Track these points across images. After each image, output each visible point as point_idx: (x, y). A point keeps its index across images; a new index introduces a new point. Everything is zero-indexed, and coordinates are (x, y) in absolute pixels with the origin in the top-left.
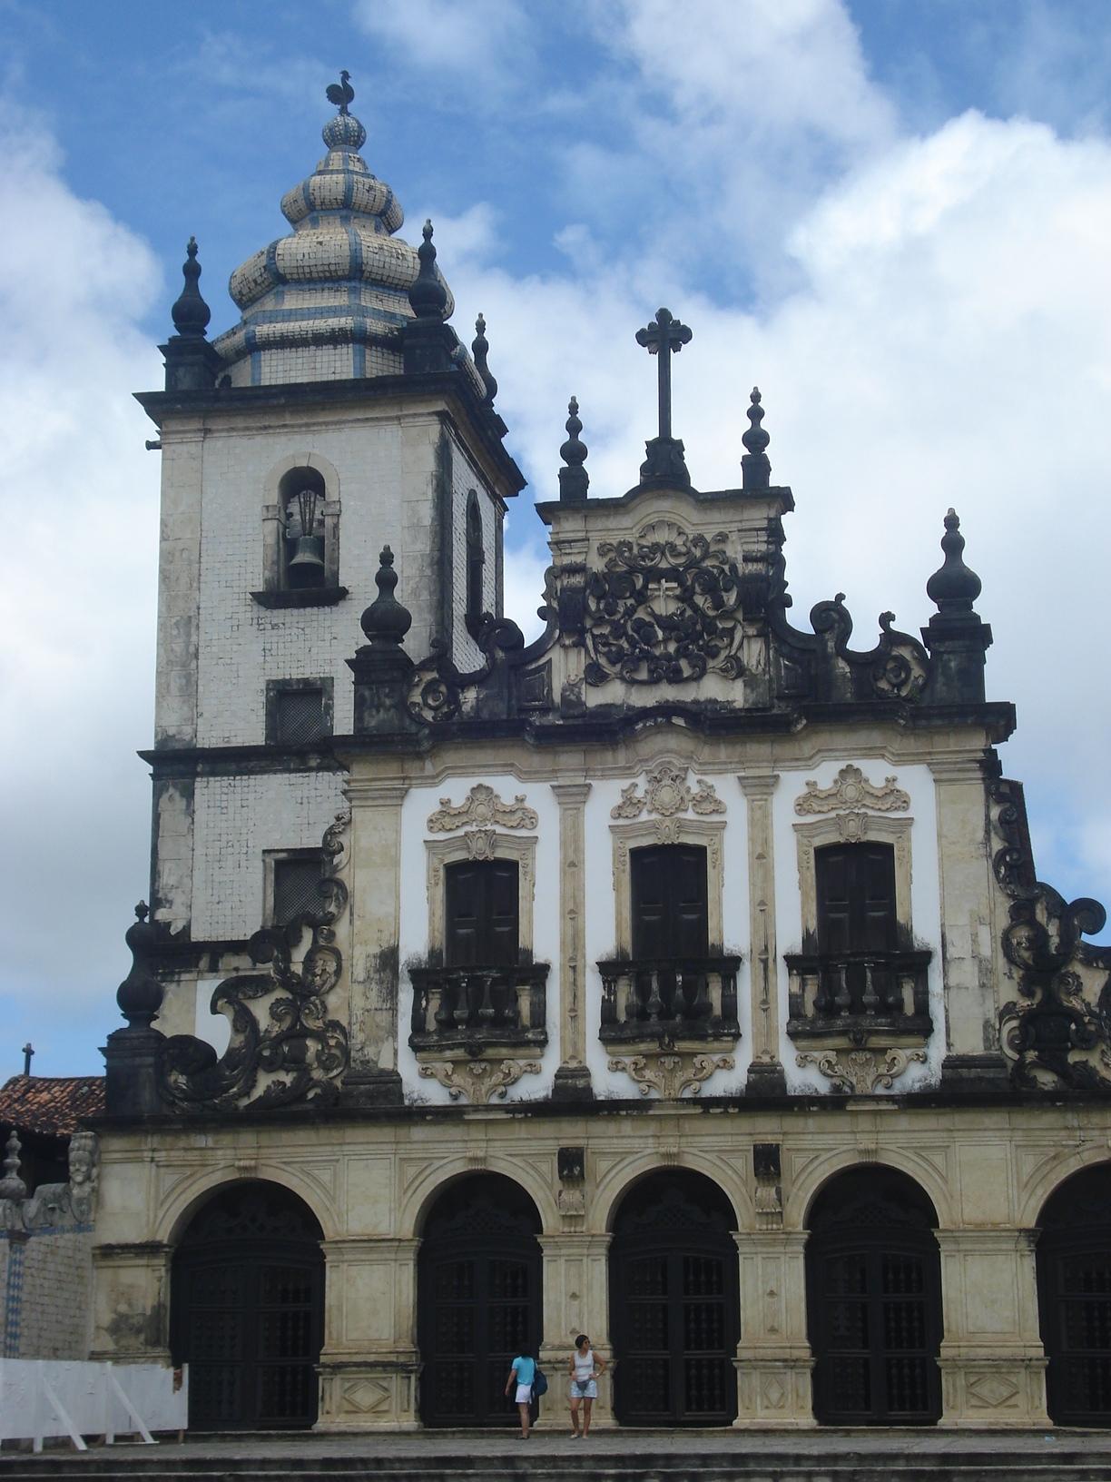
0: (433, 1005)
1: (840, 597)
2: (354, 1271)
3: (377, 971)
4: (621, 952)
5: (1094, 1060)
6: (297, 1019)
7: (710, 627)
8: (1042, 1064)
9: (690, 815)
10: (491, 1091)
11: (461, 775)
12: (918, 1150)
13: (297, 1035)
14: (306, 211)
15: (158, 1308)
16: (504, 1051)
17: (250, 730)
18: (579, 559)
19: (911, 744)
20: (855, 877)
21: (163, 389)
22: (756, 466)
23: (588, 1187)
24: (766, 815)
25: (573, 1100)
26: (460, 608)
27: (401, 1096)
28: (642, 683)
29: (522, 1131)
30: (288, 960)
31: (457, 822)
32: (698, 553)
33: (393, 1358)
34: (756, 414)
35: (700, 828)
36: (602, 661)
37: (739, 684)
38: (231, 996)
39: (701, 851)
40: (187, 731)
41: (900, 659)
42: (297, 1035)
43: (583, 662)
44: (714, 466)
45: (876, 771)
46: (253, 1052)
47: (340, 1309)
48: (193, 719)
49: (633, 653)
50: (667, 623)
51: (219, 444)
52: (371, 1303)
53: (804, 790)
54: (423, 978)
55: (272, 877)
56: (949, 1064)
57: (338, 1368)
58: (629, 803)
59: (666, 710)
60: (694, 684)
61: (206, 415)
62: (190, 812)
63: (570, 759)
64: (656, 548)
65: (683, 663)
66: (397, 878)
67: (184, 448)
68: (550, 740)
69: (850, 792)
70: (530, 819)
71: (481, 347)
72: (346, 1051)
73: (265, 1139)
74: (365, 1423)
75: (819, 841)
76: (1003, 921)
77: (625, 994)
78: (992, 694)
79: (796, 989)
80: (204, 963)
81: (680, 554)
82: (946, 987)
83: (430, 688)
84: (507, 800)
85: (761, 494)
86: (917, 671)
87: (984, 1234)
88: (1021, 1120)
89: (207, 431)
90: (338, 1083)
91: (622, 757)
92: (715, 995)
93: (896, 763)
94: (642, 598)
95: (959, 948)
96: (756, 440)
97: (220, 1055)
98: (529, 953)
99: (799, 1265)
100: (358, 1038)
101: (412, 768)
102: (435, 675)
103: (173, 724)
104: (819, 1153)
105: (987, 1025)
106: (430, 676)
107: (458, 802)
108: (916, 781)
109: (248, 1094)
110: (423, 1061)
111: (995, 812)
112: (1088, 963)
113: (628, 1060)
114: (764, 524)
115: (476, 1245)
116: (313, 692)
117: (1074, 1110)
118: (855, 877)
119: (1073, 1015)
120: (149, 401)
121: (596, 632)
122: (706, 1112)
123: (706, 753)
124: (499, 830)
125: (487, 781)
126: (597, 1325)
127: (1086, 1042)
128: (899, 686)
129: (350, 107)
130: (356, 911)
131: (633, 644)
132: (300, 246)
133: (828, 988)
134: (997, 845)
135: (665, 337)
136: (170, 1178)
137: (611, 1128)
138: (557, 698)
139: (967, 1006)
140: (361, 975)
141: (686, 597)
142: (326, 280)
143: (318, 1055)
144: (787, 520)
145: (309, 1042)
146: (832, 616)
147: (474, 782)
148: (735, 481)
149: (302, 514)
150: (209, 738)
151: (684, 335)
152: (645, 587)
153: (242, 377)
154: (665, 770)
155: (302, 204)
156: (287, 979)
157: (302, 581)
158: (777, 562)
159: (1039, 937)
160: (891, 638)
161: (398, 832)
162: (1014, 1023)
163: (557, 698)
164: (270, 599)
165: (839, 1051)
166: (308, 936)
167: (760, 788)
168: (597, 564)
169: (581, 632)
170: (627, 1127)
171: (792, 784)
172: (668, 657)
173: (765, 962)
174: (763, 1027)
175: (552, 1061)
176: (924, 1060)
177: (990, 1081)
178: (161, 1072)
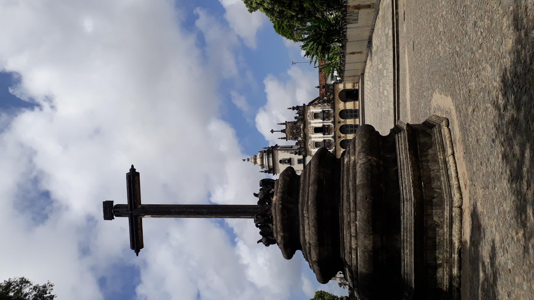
14: (255, 162)
22: (283, 124)
44: (284, 127)
45: (308, 114)
63: (307, 138)
85: (285, 124)
87: (345, 106)
96: (281, 124)
108: (309, 111)
120: (274, 175)
127: (329, 99)
139: (328, 108)
146: (296, 118)
158: (291, 122)
160: (298, 113)
171: (309, 121)
174: (329, 123)
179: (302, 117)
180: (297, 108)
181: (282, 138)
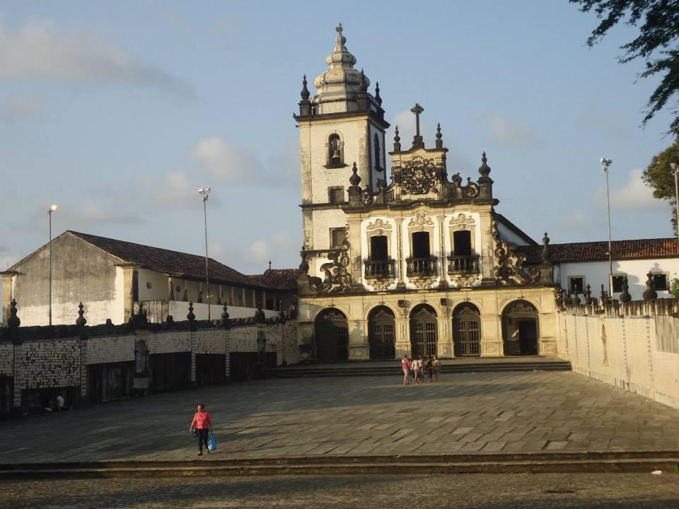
0: (370, 268)
5: (514, 278)
7: (429, 180)
10: (383, 288)
13: (339, 276)
15: (313, 336)
17: (324, 198)
19: (475, 207)
20: (462, 239)
22: (439, 143)
25: (402, 290)
26: (374, 165)
29: (390, 296)
30: (337, 259)
34: (439, 129)
39: (427, 234)
42: (339, 276)
44: (430, 142)
45: (468, 214)
46: (330, 280)
50: (418, 179)
54: (367, 263)
56: (482, 280)
59: (418, 203)
60: (425, 195)
62: (311, 219)
64: (417, 162)
68: (394, 208)
71: (377, 90)
72: (350, 279)
75: (455, 231)
76: (495, 248)
77: (412, 266)
78: (494, 197)
80: (317, 255)
83: (366, 196)
84: (384, 222)
85: (439, 146)
91: (410, 212)
94: (414, 174)
95: (486, 252)
96: (439, 136)
97: (323, 281)
98: (390, 257)
100: (353, 277)
104: (457, 298)
105: (491, 271)
106: (366, 193)
108: (476, 216)
111: (493, 223)
112: (513, 257)
116: (340, 189)
118: (462, 239)
119: (510, 269)
125: (380, 218)
128: (472, 194)
129: (342, 33)
132: (330, 77)
133: (457, 263)
134: (494, 230)
135: (418, 110)
139: (488, 269)
141: (424, 174)
145: (343, 278)
146: (457, 178)
148: (434, 146)
151: (423, 110)
155: (331, 61)
157: (335, 161)
159: (503, 250)
160: (470, 183)
168: (403, 166)
169: (400, 183)
170: (413, 295)
171: (449, 217)
172: (420, 188)
176: (478, 279)
178: (311, 284)
179: (460, 197)
180: (486, 181)
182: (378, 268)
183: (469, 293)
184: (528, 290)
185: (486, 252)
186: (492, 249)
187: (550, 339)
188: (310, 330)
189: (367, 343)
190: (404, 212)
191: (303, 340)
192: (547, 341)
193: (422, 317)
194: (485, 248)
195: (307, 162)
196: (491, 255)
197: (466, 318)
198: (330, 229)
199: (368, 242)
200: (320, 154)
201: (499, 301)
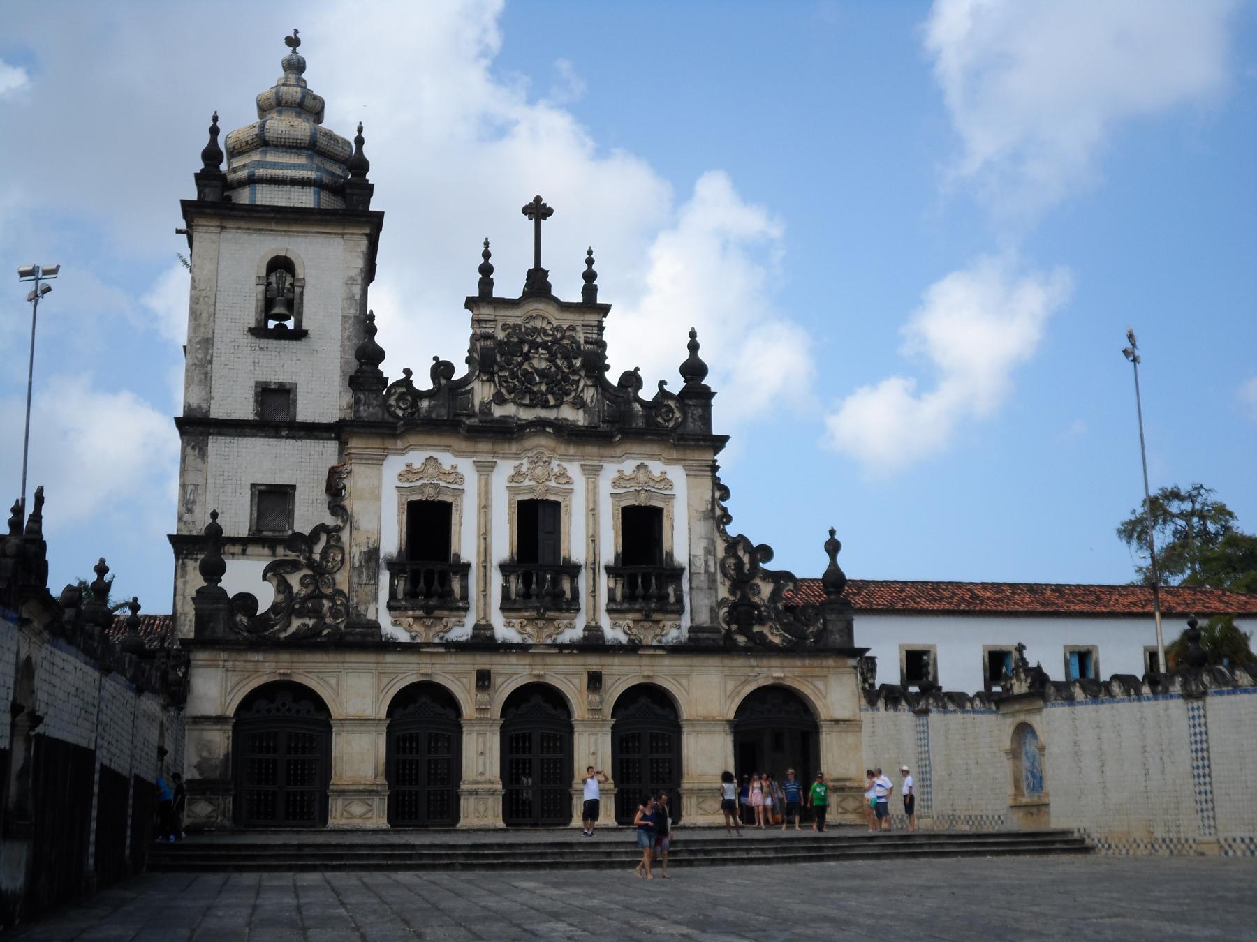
0: (401, 586)
1: (637, 369)
2: (351, 736)
3: (367, 562)
4: (512, 558)
5: (766, 630)
6: (317, 587)
7: (566, 379)
8: (740, 632)
9: (553, 483)
10: (436, 635)
11: (422, 450)
12: (674, 676)
13: (317, 596)
15: (226, 756)
16: (446, 613)
17: (245, 410)
18: (490, 331)
20: (641, 526)
21: (195, 198)
22: (590, 290)
23: (491, 691)
24: (595, 487)
25: (483, 642)
27: (381, 636)
28: (526, 406)
29: (451, 659)
30: (311, 552)
31: (416, 477)
32: (559, 336)
33: (374, 788)
35: (559, 492)
36: (503, 391)
37: (581, 411)
38: (275, 571)
39: (558, 504)
40: (204, 405)
41: (669, 406)
42: (317, 596)
43: (493, 391)
44: (568, 289)
45: (656, 468)
46: (287, 606)
47: (342, 758)
48: (209, 399)
49: (523, 390)
50: (542, 373)
51: (230, 236)
52: (359, 755)
53: (617, 475)
54: (395, 567)
55: (256, 500)
56: (691, 630)
57: (342, 793)
58: (518, 473)
59: (539, 425)
61: (223, 217)
62: (203, 454)
63: (484, 446)
65: (550, 397)
66: (379, 508)
67: (208, 236)
69: (642, 477)
70: (460, 479)
72: (346, 607)
73: (295, 658)
74: (357, 823)
75: (624, 504)
76: (721, 553)
78: (716, 431)
79: (612, 585)
81: (546, 334)
82: (691, 588)
83: (401, 397)
84: (447, 466)
85: (592, 305)
86: (677, 414)
87: (706, 723)
88: (728, 662)
89: (223, 228)
90: (342, 626)
91: (514, 448)
92: (566, 586)
93: (667, 464)
94: (527, 357)
96: (590, 276)
98: (458, 556)
99: (609, 738)
101: (389, 443)
102: (404, 390)
103: (194, 401)
104: (622, 675)
105: (713, 612)
107: (417, 465)
108: (677, 475)
109: (285, 630)
110: (393, 616)
111: (717, 494)
112: (764, 579)
113: (516, 622)
114: (596, 323)
115: (422, 722)
117: (756, 657)
118: (641, 526)
119: (756, 606)
121: (501, 374)
122: (561, 652)
123: (562, 449)
124: (442, 484)
125: (435, 455)
126: (494, 770)
127: (761, 621)
128: (668, 421)
129: (298, 49)
130: (354, 524)
131: (522, 383)
135: (538, 211)
136: (233, 679)
137: (504, 660)
138: (477, 408)
140: (357, 564)
141: (551, 360)
142: (293, 147)
143: (330, 608)
144: (607, 322)
146: (632, 379)
147: (428, 454)
148: (578, 299)
149: (278, 284)
150: (217, 412)
152: (529, 351)
153: (244, 197)
154: (539, 456)
156: (311, 564)
158: (602, 345)
160: (663, 394)
161: (380, 479)
162: (726, 609)
163: (477, 408)
164: (259, 332)
165: (635, 621)
166: (324, 538)
167: (592, 472)
168: (501, 335)
170: (513, 659)
171: (610, 471)
172: (542, 393)
173: (594, 570)
175: (471, 620)
176: (679, 627)
177: (714, 640)
178: (232, 614)
179: (640, 423)
181: (486, 270)
182: (429, 584)
183: (658, 661)
184: (798, 662)
185: (699, 563)
186: (715, 556)
187: (848, 784)
188: (220, 741)
189: (382, 780)
190: (499, 448)
191: (198, 767)
192: (842, 789)
193: (536, 723)
194: (699, 551)
195: (205, 315)
196: (712, 570)
197: (648, 726)
198: (253, 485)
199: (400, 514)
200: (243, 303)
201: (731, 685)
